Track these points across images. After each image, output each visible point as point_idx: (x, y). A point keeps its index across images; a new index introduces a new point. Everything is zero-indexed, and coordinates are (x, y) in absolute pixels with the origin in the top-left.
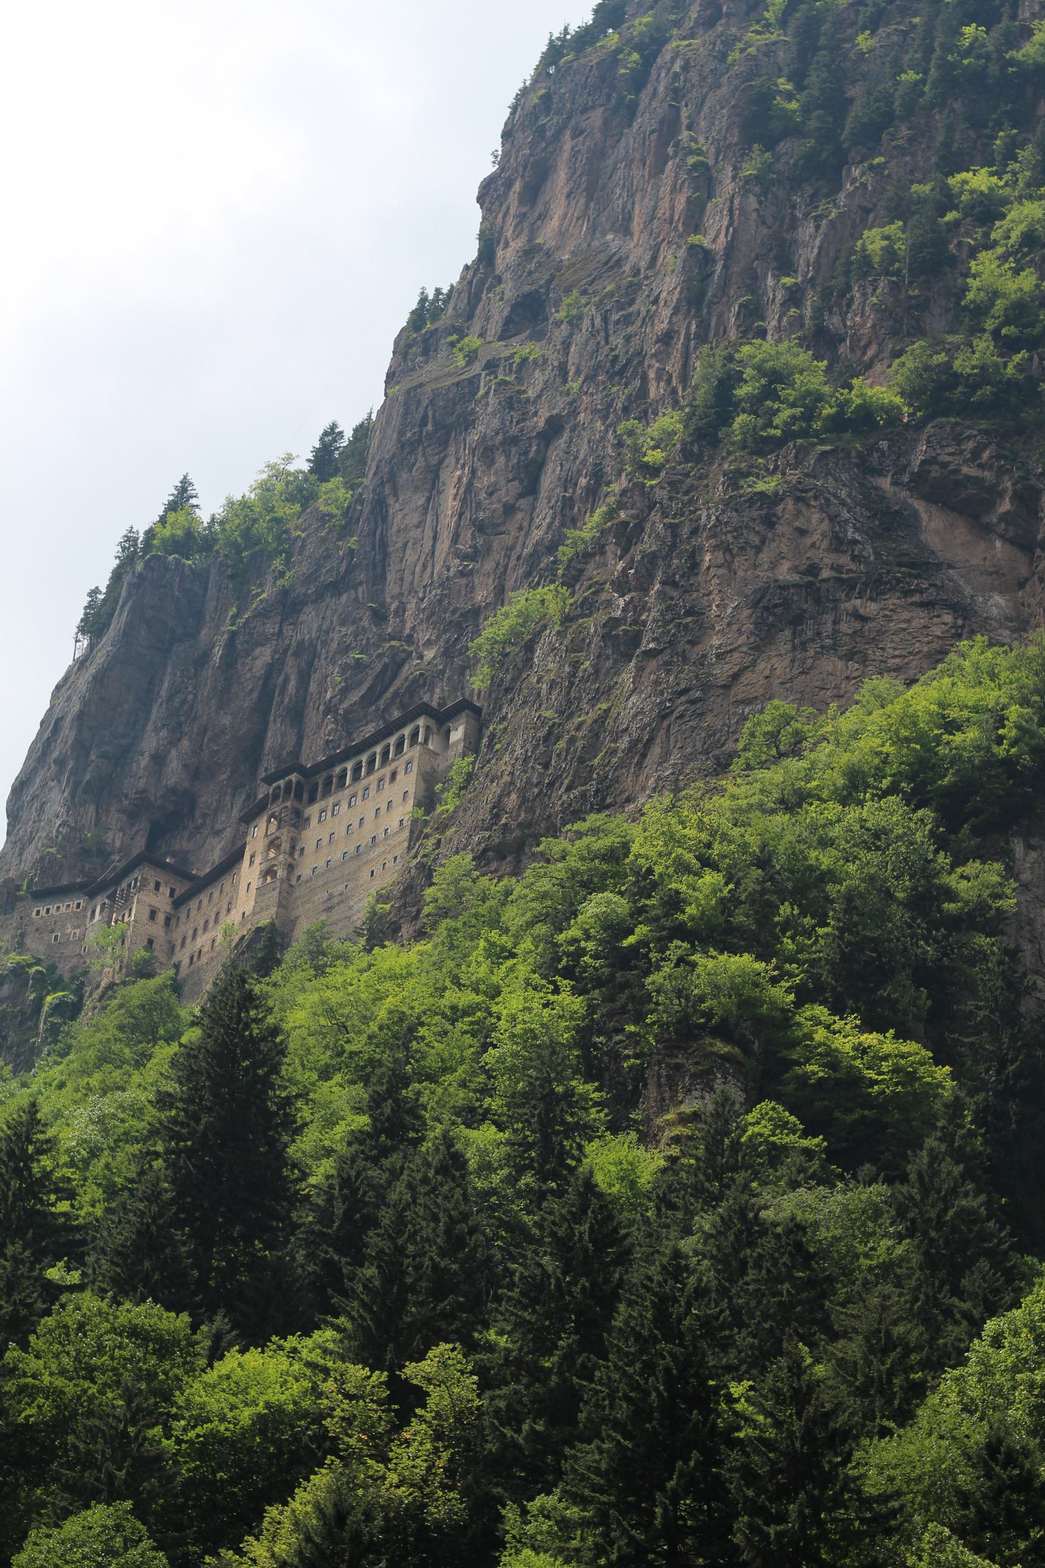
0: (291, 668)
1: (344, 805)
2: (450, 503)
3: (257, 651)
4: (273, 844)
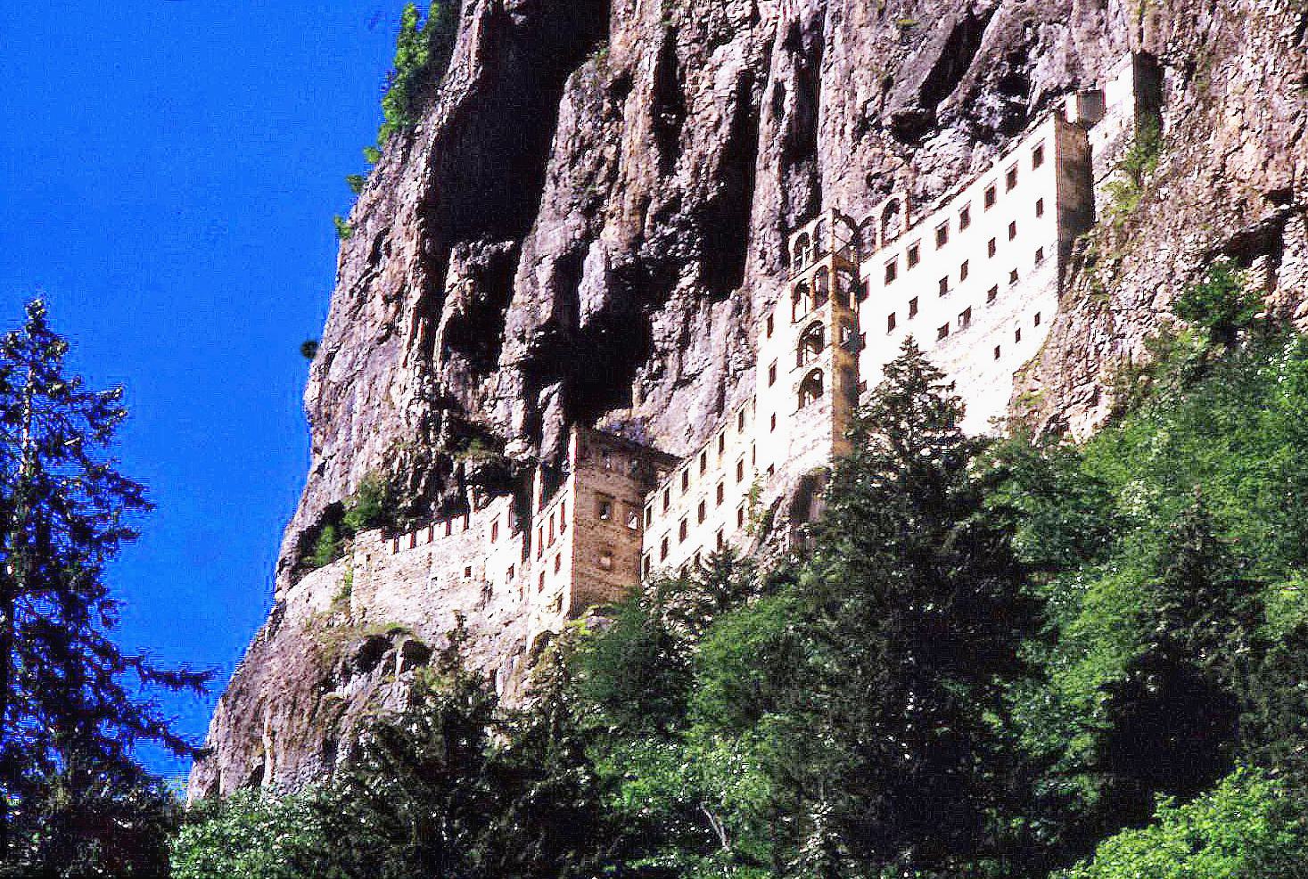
0: (782, 67)
3: (719, 52)
4: (812, 339)
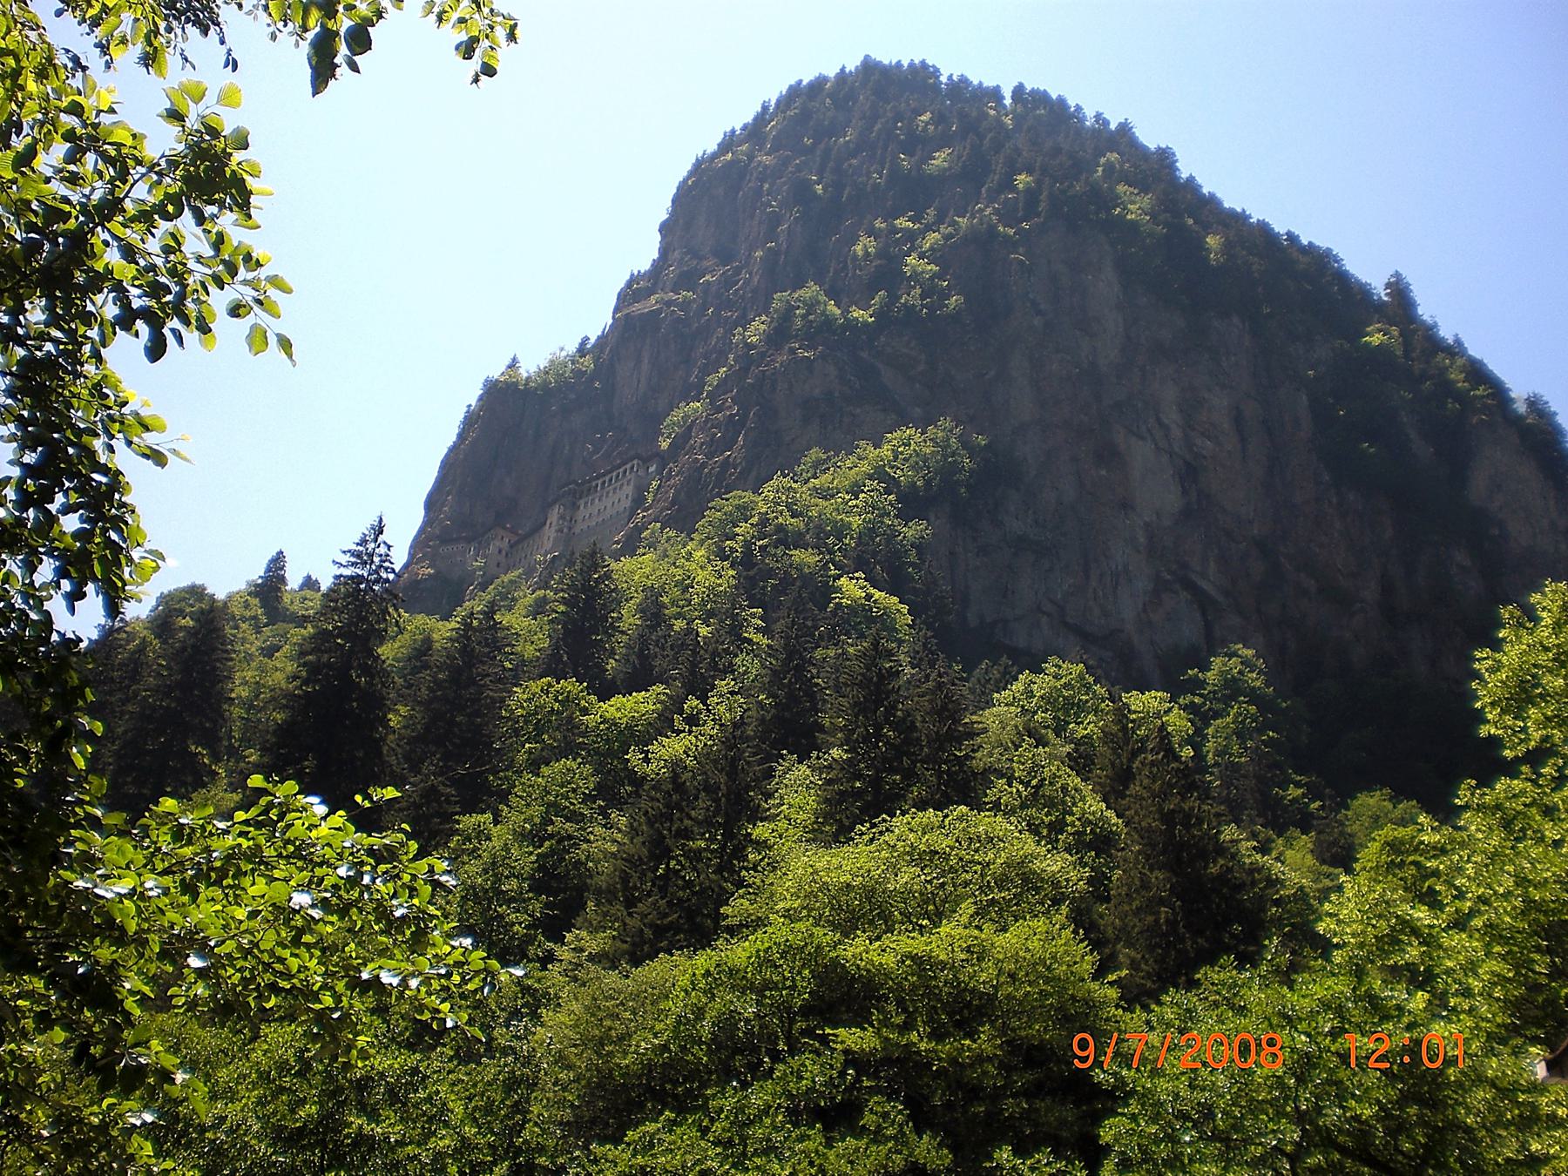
1: (597, 500)
2: (645, 366)
4: (562, 517)
